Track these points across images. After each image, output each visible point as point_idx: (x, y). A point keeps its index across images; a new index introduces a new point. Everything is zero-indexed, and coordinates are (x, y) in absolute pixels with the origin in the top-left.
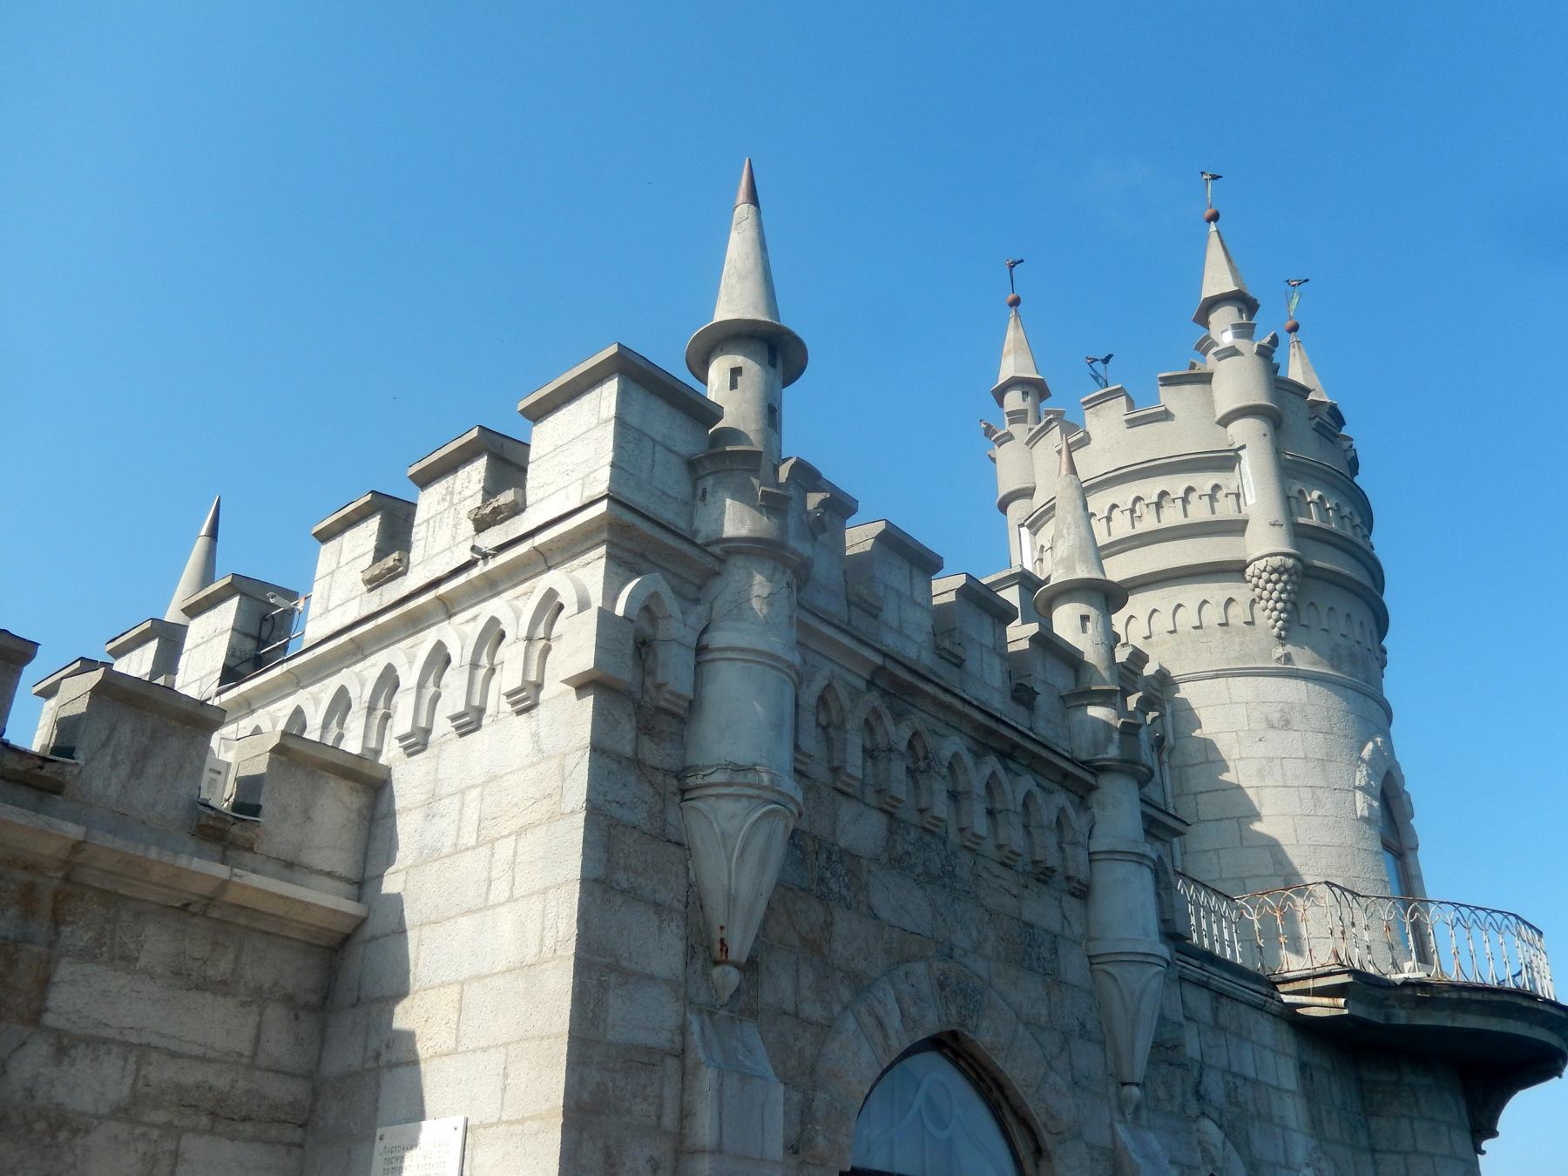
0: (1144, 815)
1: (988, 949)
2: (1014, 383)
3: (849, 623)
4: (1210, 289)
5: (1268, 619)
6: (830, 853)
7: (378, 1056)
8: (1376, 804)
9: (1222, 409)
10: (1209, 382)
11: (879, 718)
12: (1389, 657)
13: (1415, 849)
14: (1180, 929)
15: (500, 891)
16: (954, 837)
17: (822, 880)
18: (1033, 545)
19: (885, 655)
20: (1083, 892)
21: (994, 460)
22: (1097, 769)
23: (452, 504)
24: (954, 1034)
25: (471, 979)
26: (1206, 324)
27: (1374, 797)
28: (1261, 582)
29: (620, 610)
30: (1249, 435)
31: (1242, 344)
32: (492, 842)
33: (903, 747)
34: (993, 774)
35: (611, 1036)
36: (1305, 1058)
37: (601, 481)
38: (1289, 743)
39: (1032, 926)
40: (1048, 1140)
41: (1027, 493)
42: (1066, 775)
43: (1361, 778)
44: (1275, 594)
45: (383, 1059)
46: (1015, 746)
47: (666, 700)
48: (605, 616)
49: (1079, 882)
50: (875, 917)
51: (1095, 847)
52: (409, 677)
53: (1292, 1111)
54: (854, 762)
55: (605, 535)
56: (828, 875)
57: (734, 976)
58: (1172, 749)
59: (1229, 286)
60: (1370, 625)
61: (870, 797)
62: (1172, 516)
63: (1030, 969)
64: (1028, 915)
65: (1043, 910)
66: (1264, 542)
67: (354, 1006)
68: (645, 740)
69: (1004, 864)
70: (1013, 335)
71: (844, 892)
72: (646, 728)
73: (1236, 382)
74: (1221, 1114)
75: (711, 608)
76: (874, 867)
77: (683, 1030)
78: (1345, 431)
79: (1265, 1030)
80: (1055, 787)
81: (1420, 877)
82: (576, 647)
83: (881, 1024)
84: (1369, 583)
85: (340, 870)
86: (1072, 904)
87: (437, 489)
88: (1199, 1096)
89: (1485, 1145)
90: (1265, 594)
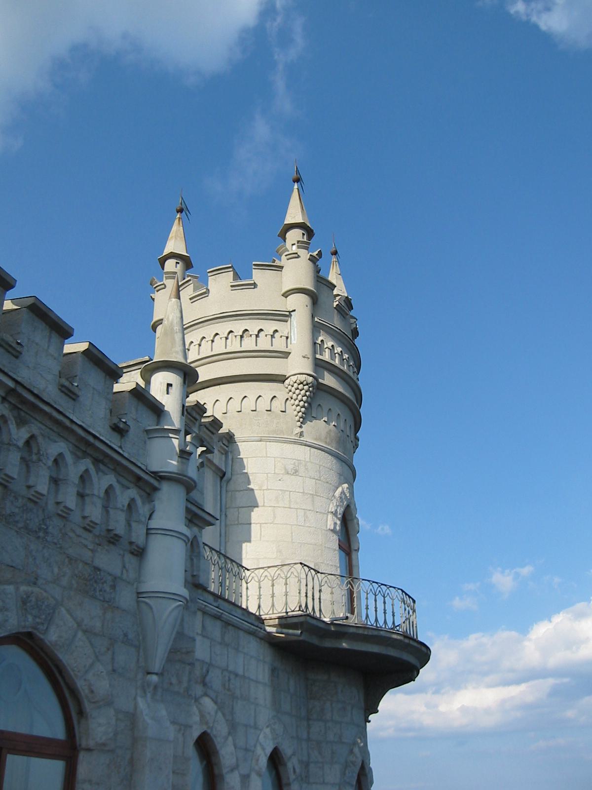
0: (188, 510)
1: (65, 581)
2: (172, 255)
4: (289, 220)
5: (294, 411)
8: (338, 522)
14: (202, 581)
16: (51, 507)
19: (17, 382)
20: (140, 553)
21: (153, 299)
22: (160, 477)
24: (30, 635)
27: (338, 518)
30: (300, 304)
33: (21, 443)
34: (87, 471)
39: (99, 570)
40: (87, 706)
42: (139, 478)
44: (300, 397)
46: (107, 456)
49: (137, 546)
51: (153, 524)
53: (262, 694)
58: (229, 481)
59: (299, 219)
60: (351, 422)
62: (249, 344)
63: (94, 597)
64: (97, 563)
65: (109, 561)
66: (298, 366)
69: (85, 529)
70: (177, 229)
73: (296, 272)
78: (352, 313)
79: (253, 647)
80: (131, 485)
88: (204, 684)
89: (371, 717)
90: (294, 396)
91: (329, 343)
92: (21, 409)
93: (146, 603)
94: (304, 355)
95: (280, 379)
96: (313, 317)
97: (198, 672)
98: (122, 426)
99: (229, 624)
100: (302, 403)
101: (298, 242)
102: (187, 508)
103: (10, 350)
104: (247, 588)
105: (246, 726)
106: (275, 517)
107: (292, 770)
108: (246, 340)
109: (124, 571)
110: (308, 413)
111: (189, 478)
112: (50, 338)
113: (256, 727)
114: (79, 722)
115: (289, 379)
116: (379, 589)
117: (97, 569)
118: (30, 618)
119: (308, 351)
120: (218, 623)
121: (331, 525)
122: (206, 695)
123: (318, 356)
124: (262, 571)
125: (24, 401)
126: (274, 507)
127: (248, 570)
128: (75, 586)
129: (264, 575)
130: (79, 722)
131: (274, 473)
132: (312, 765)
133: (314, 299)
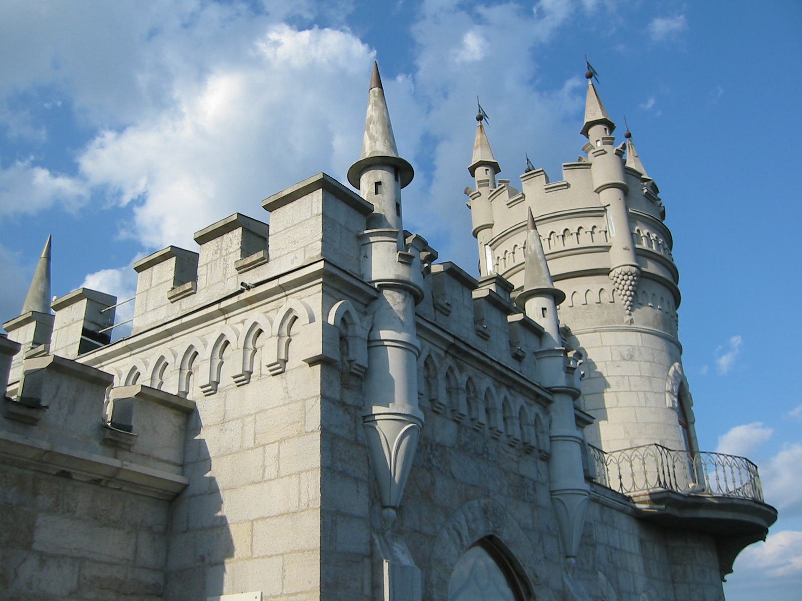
0: (576, 415)
2: (481, 164)
3: (435, 320)
4: (589, 118)
5: (622, 300)
7: (203, 559)
8: (676, 400)
9: (598, 184)
13: (693, 423)
14: (591, 474)
15: (271, 472)
16: (488, 433)
18: (493, 258)
20: (546, 458)
21: (470, 207)
22: (552, 391)
23: (221, 256)
25: (257, 519)
26: (587, 136)
27: (675, 396)
28: (619, 280)
29: (331, 320)
30: (611, 198)
31: (607, 148)
32: (264, 445)
33: (464, 386)
37: (316, 249)
38: (631, 368)
40: (535, 589)
41: (490, 226)
42: (538, 396)
43: (668, 387)
44: (626, 287)
45: (207, 561)
46: (515, 382)
47: (355, 369)
48: (325, 324)
49: (546, 453)
50: (454, 478)
51: (554, 433)
52: (205, 354)
53: (636, 563)
54: (443, 397)
55: (321, 280)
57: (392, 512)
59: (600, 116)
61: (449, 415)
62: (571, 242)
65: (529, 468)
66: (620, 258)
67: (185, 532)
68: (345, 391)
69: (511, 445)
72: (345, 385)
73: (604, 169)
75: (374, 317)
77: (372, 543)
78: (659, 195)
79: (625, 523)
80: (533, 402)
81: (696, 438)
82: (310, 341)
83: (459, 534)
84: (671, 280)
85: (173, 459)
86: (542, 465)
87: (212, 245)
89: (727, 577)
90: (621, 287)
91: (645, 232)
92: (458, 358)
93: (558, 499)
94: (624, 247)
95: (606, 272)
96: (627, 209)
98: (520, 354)
100: (628, 293)
101: (603, 139)
103: (443, 311)
104: (608, 470)
108: (568, 239)
110: (635, 302)
115: (613, 271)
116: (726, 460)
117: (523, 477)
118: (491, 523)
119: (627, 243)
120: (597, 506)
121: (669, 403)
123: (637, 246)
125: (459, 351)
126: (616, 392)
127: (606, 453)
129: (621, 458)
131: (612, 361)
133: (624, 189)
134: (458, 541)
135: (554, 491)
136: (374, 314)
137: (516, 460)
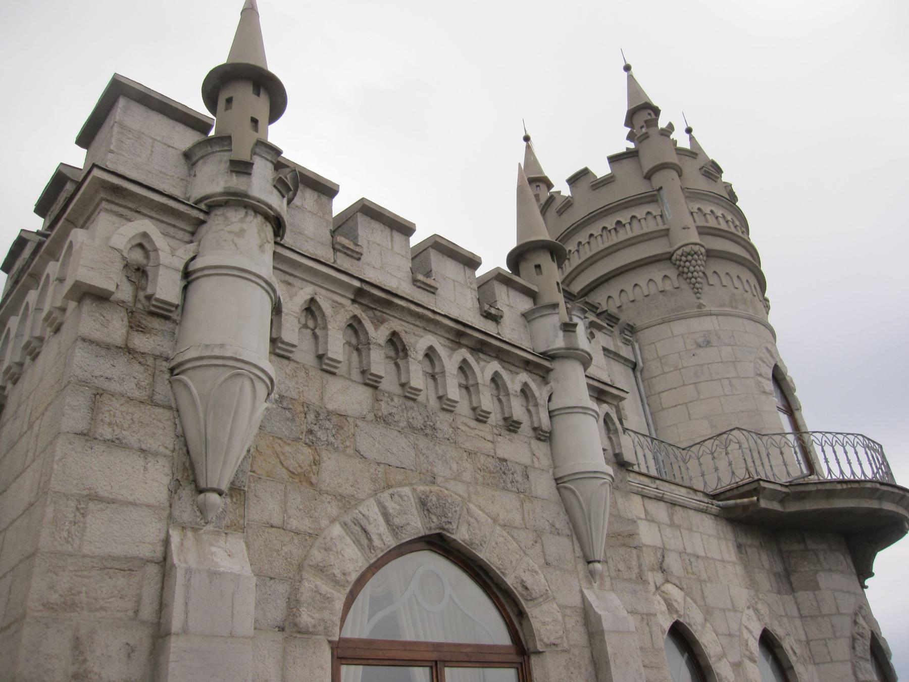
0: (590, 387)
1: (467, 476)
3: (335, 261)
6: (318, 415)
10: (637, 156)
11: (360, 322)
12: (771, 304)
13: (799, 409)
17: (310, 432)
24: (440, 536)
35: (86, 549)
36: (740, 540)
39: (506, 460)
47: (155, 306)
51: (553, 406)
56: (316, 428)
60: (753, 281)
64: (501, 453)
71: (332, 439)
74: (680, 582)
75: (199, 245)
76: (360, 423)
77: (167, 542)
86: (541, 449)
88: (663, 571)
92: (376, 309)
93: (566, 488)
97: (649, 558)
98: (493, 311)
99: (675, 505)
102: (588, 384)
105: (723, 610)
106: (699, 393)
107: (790, 651)
109: (535, 460)
111: (582, 350)
112: (392, 237)
113: (734, 609)
114: (521, 624)
116: (835, 439)
118: (435, 519)
120: (662, 504)
122: (667, 581)
124: (698, 446)
128: (481, 480)
130: (521, 624)
132: (811, 643)
134: (365, 542)
135: (560, 478)
136: (200, 241)
137: (490, 438)
